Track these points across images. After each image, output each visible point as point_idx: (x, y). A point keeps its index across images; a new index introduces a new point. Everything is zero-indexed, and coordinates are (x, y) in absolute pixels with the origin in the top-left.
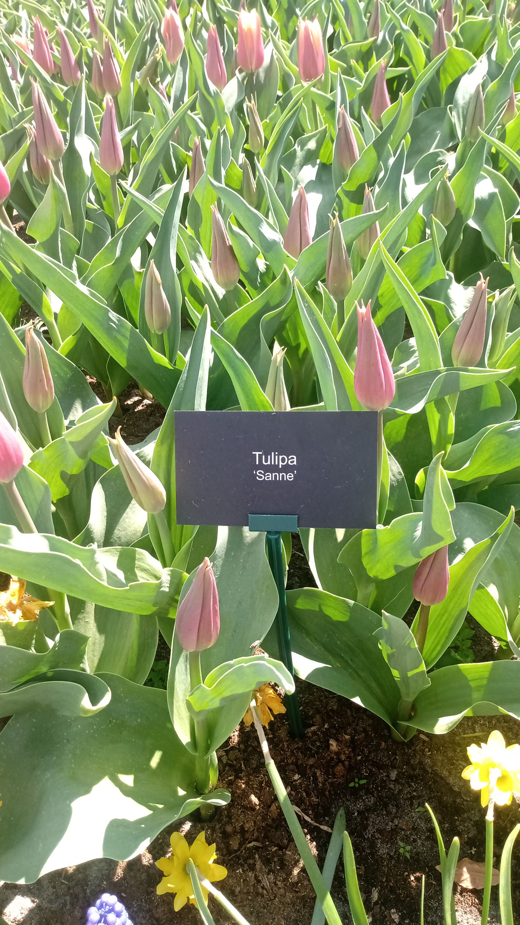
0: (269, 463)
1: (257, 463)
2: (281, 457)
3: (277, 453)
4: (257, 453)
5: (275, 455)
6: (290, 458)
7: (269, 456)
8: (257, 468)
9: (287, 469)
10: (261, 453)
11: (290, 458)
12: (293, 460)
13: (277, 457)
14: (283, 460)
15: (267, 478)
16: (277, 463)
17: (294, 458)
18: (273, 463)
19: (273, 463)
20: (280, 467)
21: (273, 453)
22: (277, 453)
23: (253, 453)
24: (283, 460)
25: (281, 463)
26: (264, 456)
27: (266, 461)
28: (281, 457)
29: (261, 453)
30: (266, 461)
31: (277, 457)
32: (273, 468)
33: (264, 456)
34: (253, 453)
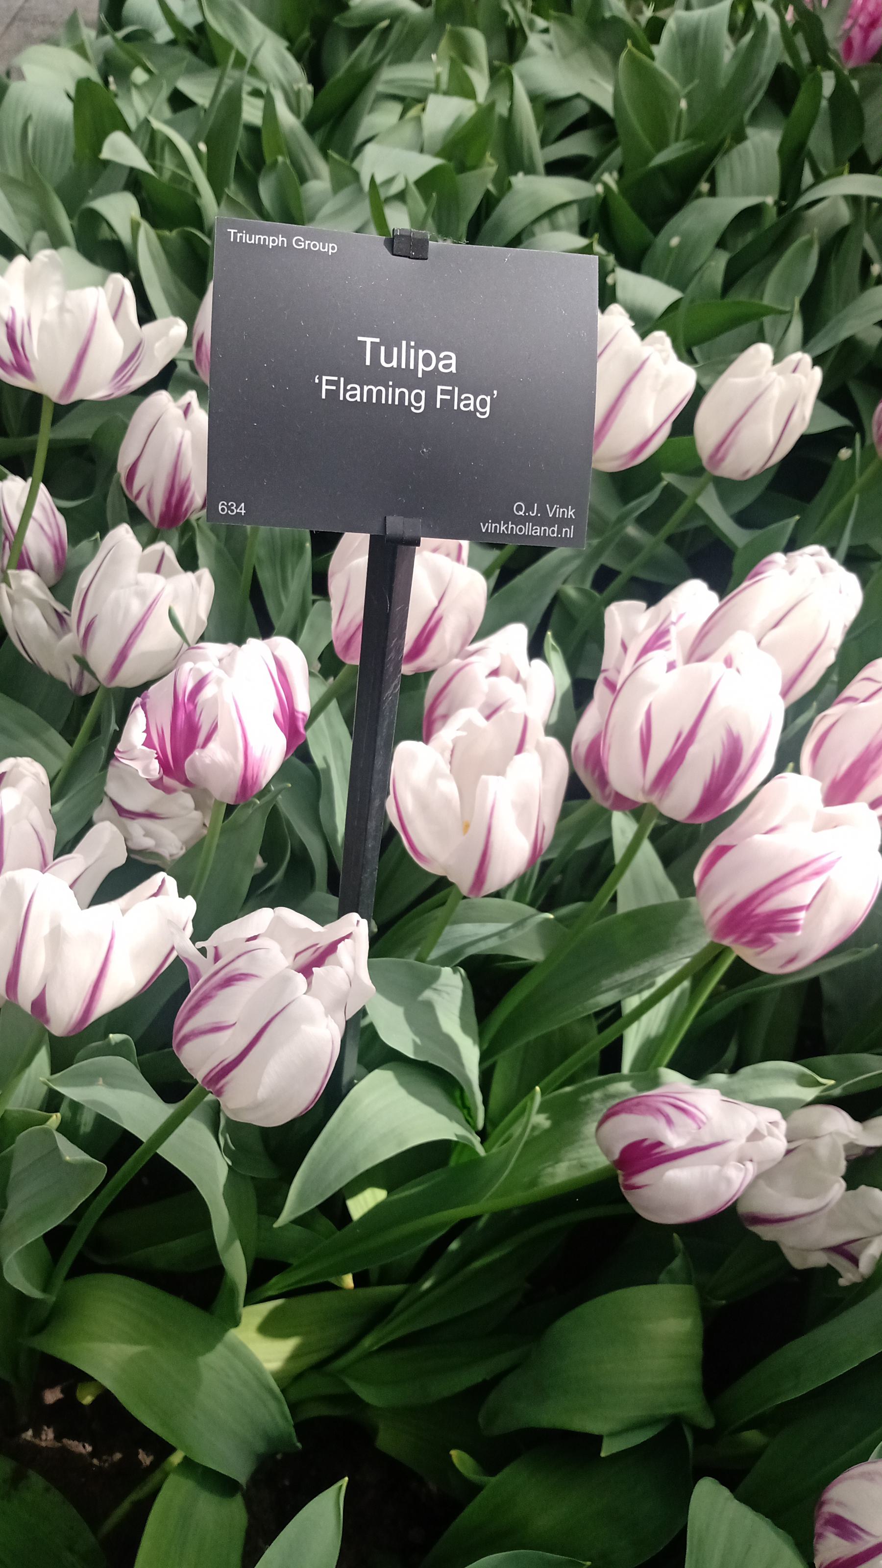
0: (394, 364)
1: (368, 363)
3: (413, 344)
4: (369, 340)
5: (408, 347)
6: (441, 356)
7: (395, 350)
10: (378, 340)
11: (441, 356)
12: (449, 363)
13: (412, 351)
14: (427, 360)
15: (465, 406)
16: (412, 367)
17: (450, 358)
18: (403, 366)
19: (403, 366)
20: (420, 375)
21: (404, 343)
22: (413, 344)
23: (360, 338)
24: (427, 360)
25: (421, 366)
26: (383, 348)
27: (389, 359)
28: (421, 353)
29: (378, 340)
30: (389, 359)
31: (412, 351)
32: (404, 378)
33: (383, 348)
34: (360, 338)
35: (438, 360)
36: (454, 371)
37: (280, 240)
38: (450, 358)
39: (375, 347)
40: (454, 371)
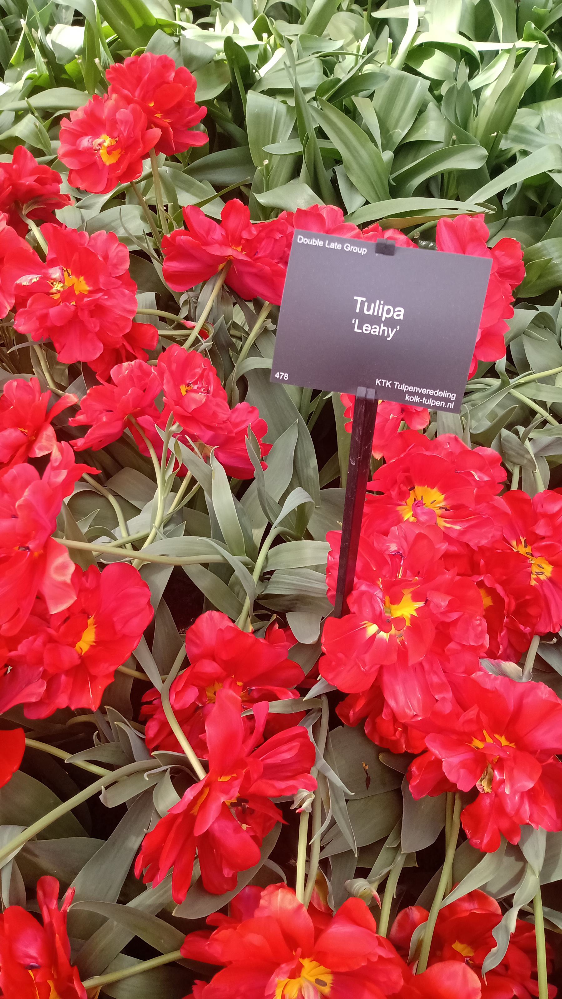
1: (358, 311)
2: (386, 307)
3: (382, 302)
4: (360, 299)
5: (380, 304)
7: (373, 305)
8: (357, 316)
9: (391, 323)
10: (364, 299)
11: (397, 309)
12: (399, 314)
13: (381, 306)
14: (388, 311)
16: (380, 315)
17: (399, 311)
18: (375, 314)
19: (375, 314)
20: (383, 319)
21: (378, 302)
22: (382, 302)
23: (356, 298)
24: (388, 311)
25: (385, 315)
26: (366, 304)
27: (368, 310)
29: (364, 299)
30: (368, 310)
31: (381, 306)
32: (375, 320)
33: (366, 304)
34: (356, 298)
35: (394, 312)
36: (402, 319)
37: (321, 244)
38: (399, 311)
39: (363, 303)
40: (402, 319)
